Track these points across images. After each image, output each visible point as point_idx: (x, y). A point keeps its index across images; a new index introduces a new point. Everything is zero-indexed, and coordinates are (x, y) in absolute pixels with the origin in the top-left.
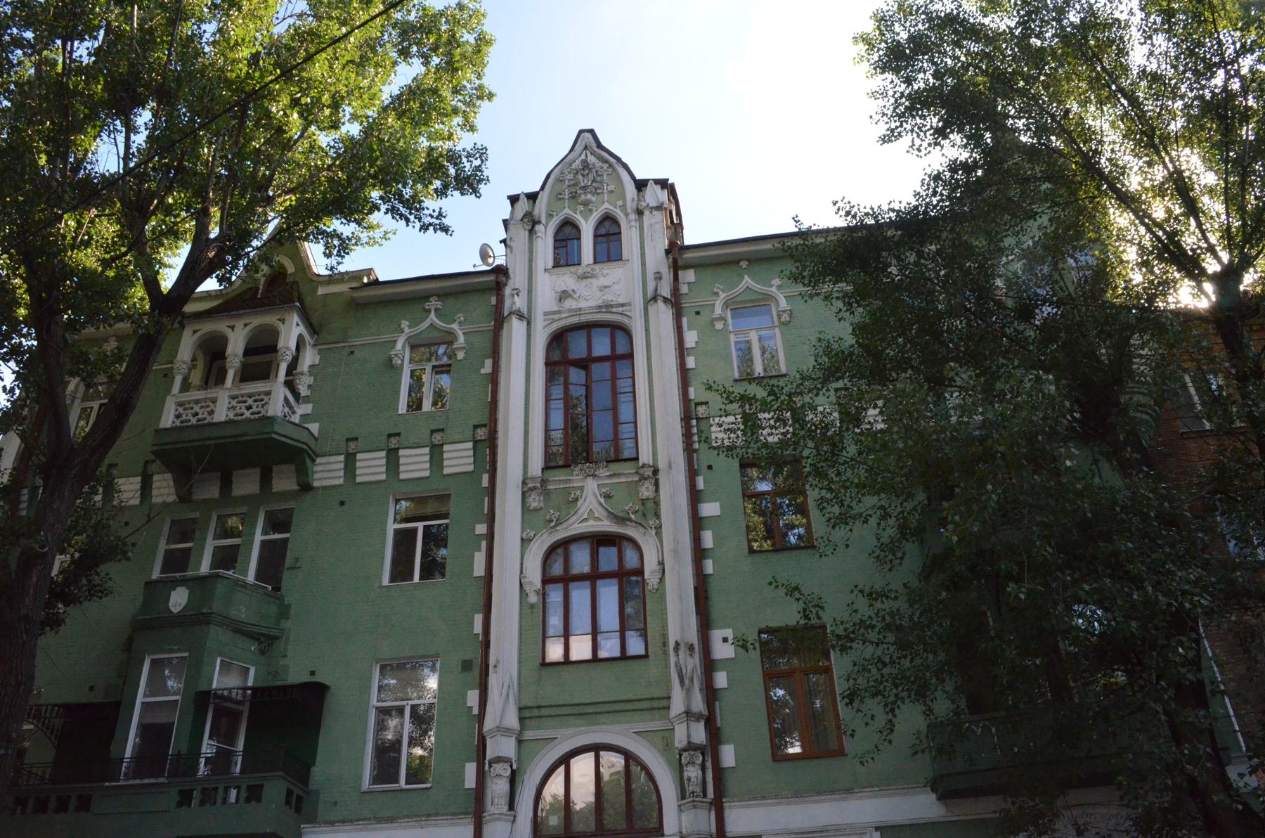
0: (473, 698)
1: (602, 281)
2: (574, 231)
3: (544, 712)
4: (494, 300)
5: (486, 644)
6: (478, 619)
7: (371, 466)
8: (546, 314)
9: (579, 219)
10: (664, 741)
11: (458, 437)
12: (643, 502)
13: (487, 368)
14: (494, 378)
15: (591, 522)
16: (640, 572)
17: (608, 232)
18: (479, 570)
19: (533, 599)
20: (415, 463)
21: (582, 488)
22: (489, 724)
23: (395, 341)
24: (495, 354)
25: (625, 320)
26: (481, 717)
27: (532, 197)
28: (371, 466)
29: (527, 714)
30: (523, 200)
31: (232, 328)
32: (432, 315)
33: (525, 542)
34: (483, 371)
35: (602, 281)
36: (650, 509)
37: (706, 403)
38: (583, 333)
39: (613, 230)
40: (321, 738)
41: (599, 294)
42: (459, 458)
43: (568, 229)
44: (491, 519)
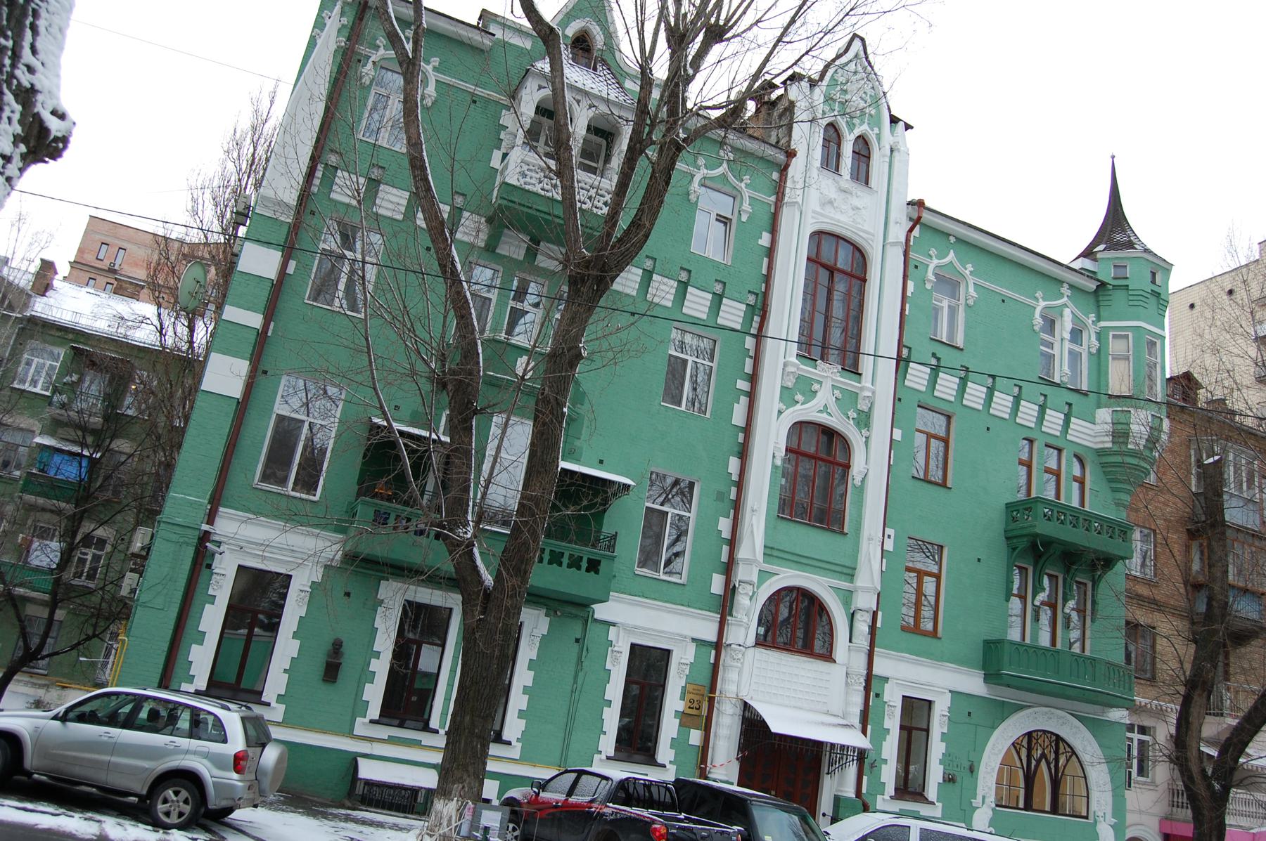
0: (724, 525)
1: (856, 202)
2: (835, 135)
3: (775, 553)
4: (775, 176)
5: (740, 484)
6: (734, 464)
7: (663, 291)
8: (814, 212)
9: (842, 123)
10: (847, 597)
11: (737, 295)
12: (860, 412)
13: (765, 240)
14: (771, 252)
15: (825, 415)
16: (847, 467)
17: (863, 151)
18: (738, 418)
19: (779, 462)
20: (697, 303)
21: (820, 383)
22: (742, 553)
23: (693, 176)
24: (774, 231)
25: (868, 248)
26: (732, 543)
27: (813, 84)
28: (663, 291)
29: (771, 552)
30: (805, 84)
31: (578, 102)
32: (725, 165)
33: (780, 412)
34: (760, 242)
35: (856, 202)
36: (864, 420)
37: (910, 349)
38: (833, 240)
39: (864, 152)
40: (605, 521)
41: (851, 213)
42: (733, 313)
43: (832, 131)
44: (753, 378)
